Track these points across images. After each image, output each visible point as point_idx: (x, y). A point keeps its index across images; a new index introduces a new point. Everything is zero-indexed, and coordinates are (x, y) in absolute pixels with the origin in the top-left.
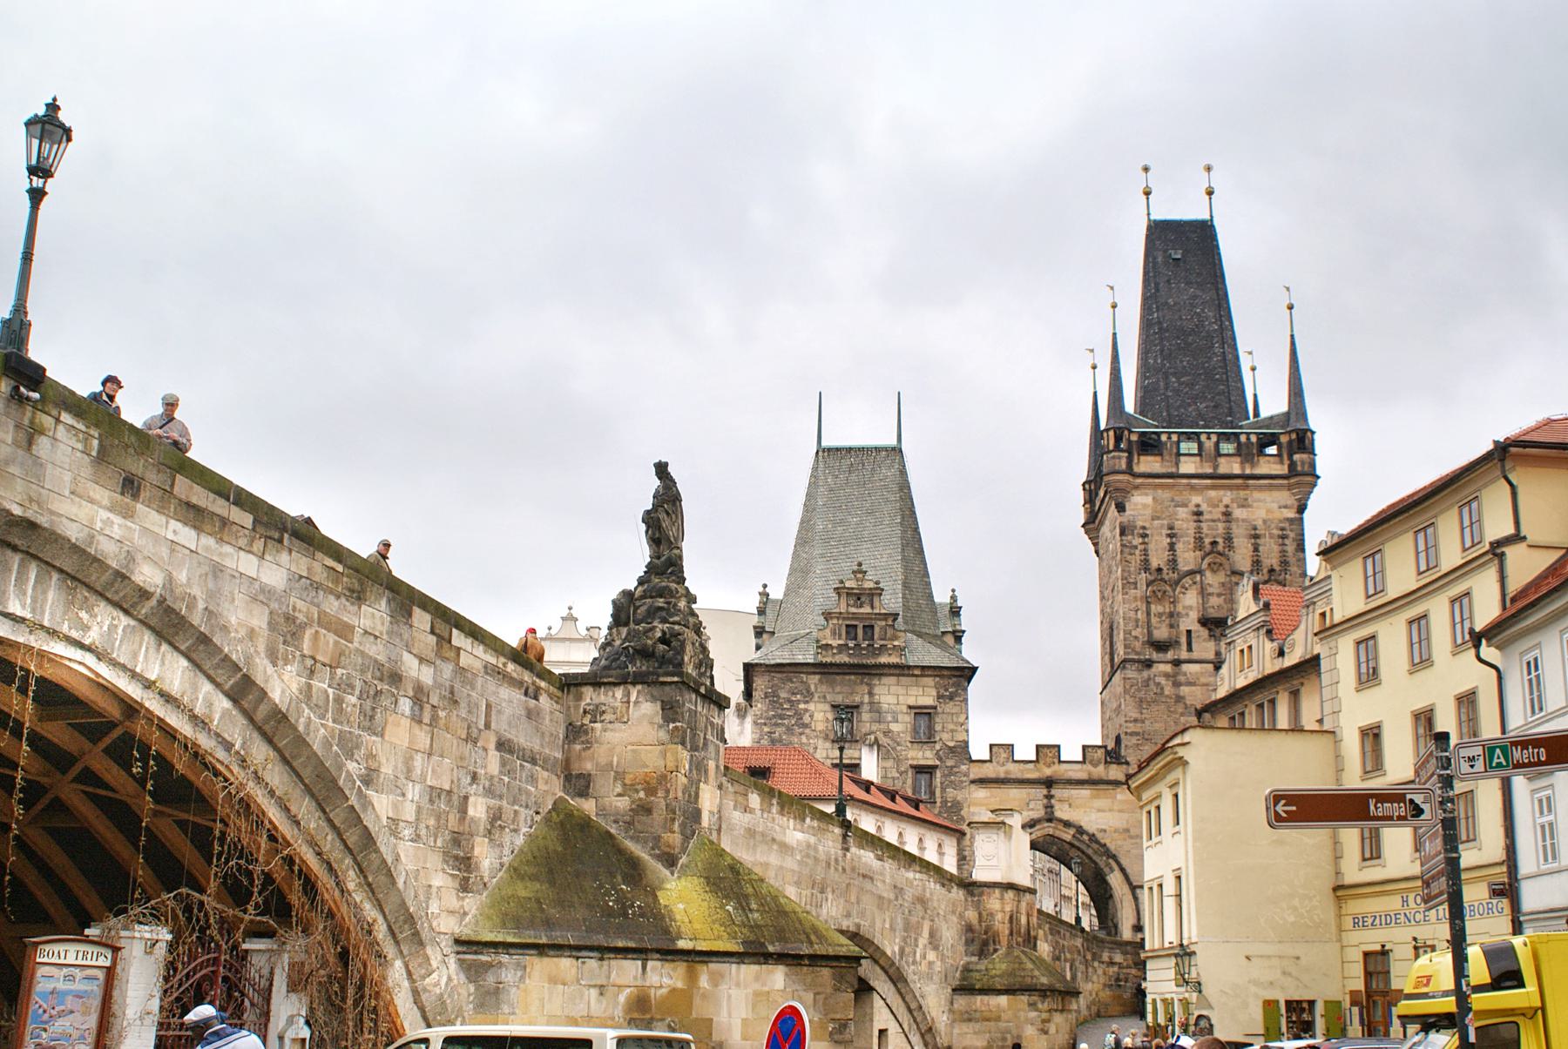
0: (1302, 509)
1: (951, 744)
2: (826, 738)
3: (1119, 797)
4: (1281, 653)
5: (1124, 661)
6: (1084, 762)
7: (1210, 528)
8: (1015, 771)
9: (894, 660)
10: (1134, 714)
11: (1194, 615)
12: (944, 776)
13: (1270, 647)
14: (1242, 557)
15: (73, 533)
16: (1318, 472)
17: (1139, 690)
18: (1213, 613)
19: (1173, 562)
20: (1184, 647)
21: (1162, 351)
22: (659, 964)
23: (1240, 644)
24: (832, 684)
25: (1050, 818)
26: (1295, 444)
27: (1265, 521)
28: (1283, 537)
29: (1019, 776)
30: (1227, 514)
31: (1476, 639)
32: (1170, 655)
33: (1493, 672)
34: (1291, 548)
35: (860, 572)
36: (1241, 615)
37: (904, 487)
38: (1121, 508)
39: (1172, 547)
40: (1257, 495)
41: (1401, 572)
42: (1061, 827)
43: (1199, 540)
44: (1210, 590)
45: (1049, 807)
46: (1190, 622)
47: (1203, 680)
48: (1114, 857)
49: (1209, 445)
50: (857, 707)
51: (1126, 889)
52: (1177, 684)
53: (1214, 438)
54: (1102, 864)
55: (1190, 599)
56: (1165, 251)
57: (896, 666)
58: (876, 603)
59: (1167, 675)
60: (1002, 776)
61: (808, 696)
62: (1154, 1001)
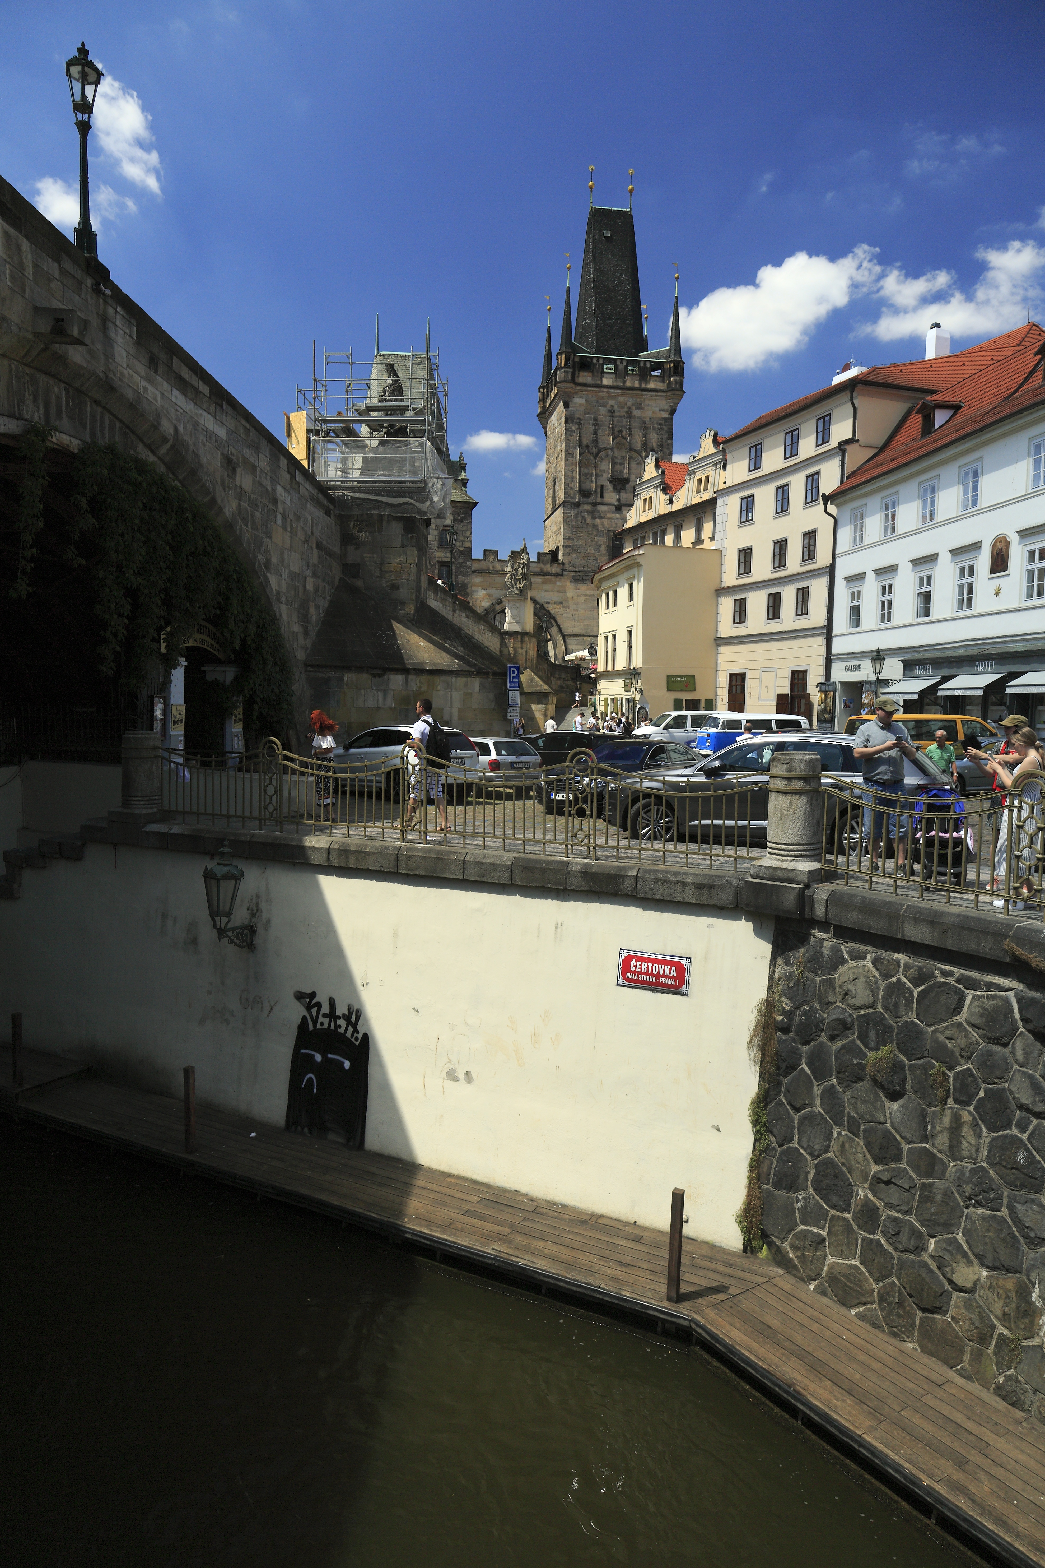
0: (673, 412)
1: (462, 549)
3: (558, 583)
4: (671, 502)
5: (564, 502)
6: (539, 562)
10: (568, 535)
13: (664, 498)
15: (130, 395)
17: (571, 520)
19: (596, 441)
21: (595, 301)
22: (414, 677)
23: (645, 495)
27: (650, 419)
31: (826, 499)
32: (590, 500)
33: (833, 520)
34: (665, 436)
36: (646, 477)
38: (566, 405)
39: (595, 433)
40: (647, 402)
41: (773, 458)
44: (616, 461)
47: (609, 516)
48: (554, 618)
52: (594, 518)
53: (625, 363)
59: (588, 512)
62: (606, 699)
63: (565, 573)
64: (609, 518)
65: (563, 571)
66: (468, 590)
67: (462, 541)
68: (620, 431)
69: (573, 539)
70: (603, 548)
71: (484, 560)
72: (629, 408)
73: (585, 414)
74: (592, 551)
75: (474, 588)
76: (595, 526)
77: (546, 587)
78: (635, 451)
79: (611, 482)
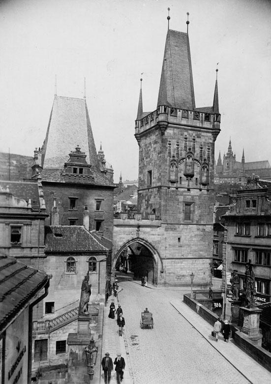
0: (214, 141)
11: (182, 172)
16: (221, 128)
19: (178, 154)
20: (179, 183)
29: (128, 224)
30: (194, 140)
35: (78, 150)
40: (203, 134)
43: (186, 147)
44: (188, 164)
46: (181, 174)
47: (184, 194)
52: (177, 195)
54: (152, 252)
59: (173, 191)
63: (162, 225)
72: (194, 137)
77: (153, 232)
78: (197, 160)
79: (185, 175)
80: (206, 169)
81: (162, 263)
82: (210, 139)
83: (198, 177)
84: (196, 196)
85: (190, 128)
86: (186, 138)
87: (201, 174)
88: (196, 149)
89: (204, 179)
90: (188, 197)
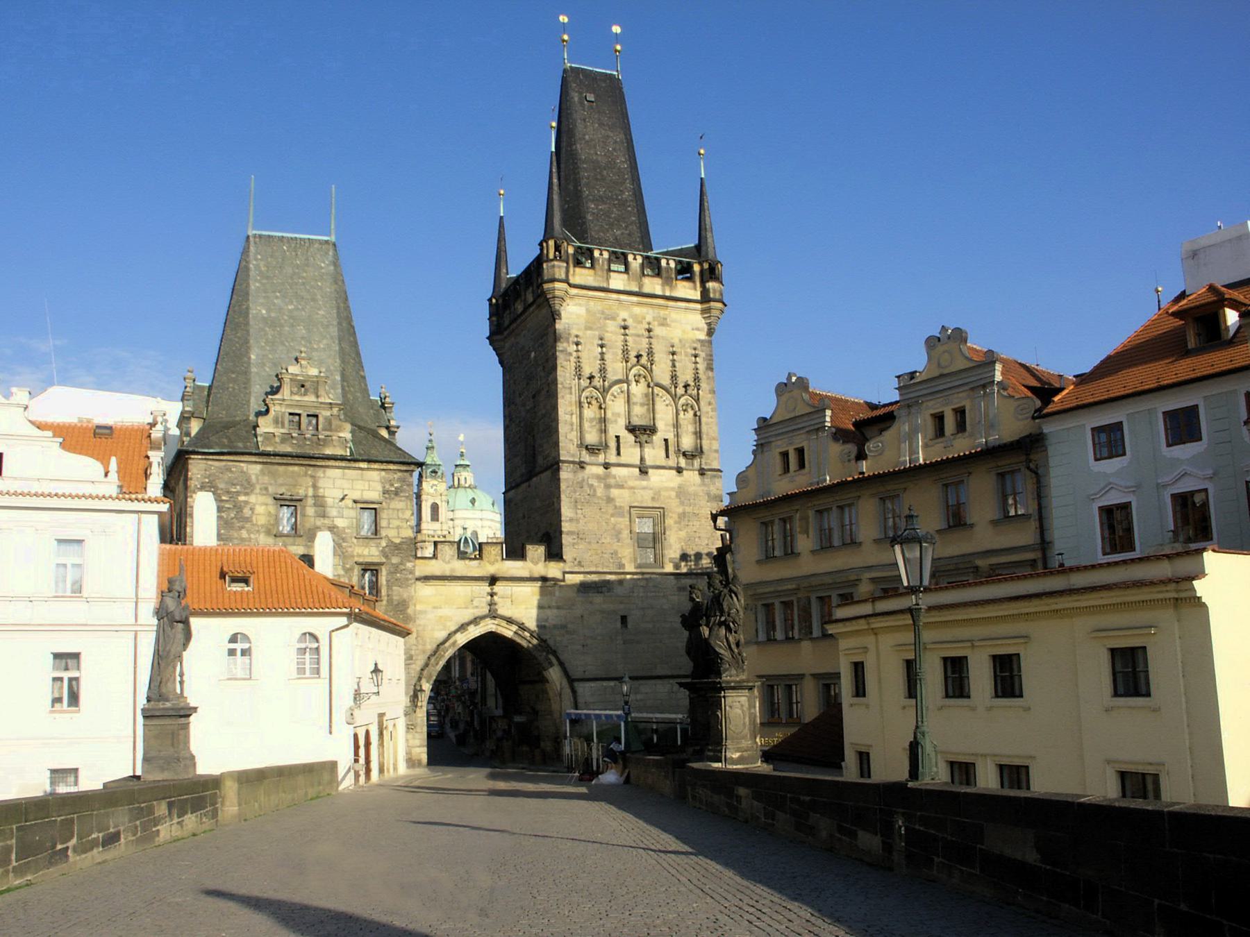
1: (397, 541)
2: (268, 532)
3: (557, 594)
7: (635, 342)
8: (461, 567)
9: (339, 452)
11: (622, 422)
12: (390, 573)
14: (662, 372)
18: (636, 421)
19: (603, 370)
20: (614, 451)
24: (273, 475)
25: (493, 614)
26: (707, 274)
28: (696, 356)
30: (649, 331)
32: (601, 458)
34: (702, 366)
37: (338, 279)
42: (504, 623)
43: (625, 351)
44: (634, 399)
45: (491, 604)
46: (617, 428)
47: (631, 483)
48: (554, 653)
49: (636, 262)
50: (300, 500)
51: (565, 682)
52: (608, 487)
53: (640, 260)
55: (616, 406)
56: (581, 93)
57: (343, 459)
58: (321, 392)
59: (598, 477)
60: (448, 573)
61: (248, 487)
64: (632, 488)
65: (564, 573)
66: (410, 611)
67: (398, 527)
68: (638, 357)
69: (578, 521)
70: (626, 533)
71: (435, 557)
73: (588, 328)
74: (608, 540)
75: (418, 607)
76: (610, 500)
80: (691, 413)
81: (574, 692)
82: (698, 329)
83: (671, 436)
84: (667, 489)
85: (635, 299)
86: (625, 328)
87: (677, 425)
88: (657, 358)
89: (687, 442)
90: (642, 492)
